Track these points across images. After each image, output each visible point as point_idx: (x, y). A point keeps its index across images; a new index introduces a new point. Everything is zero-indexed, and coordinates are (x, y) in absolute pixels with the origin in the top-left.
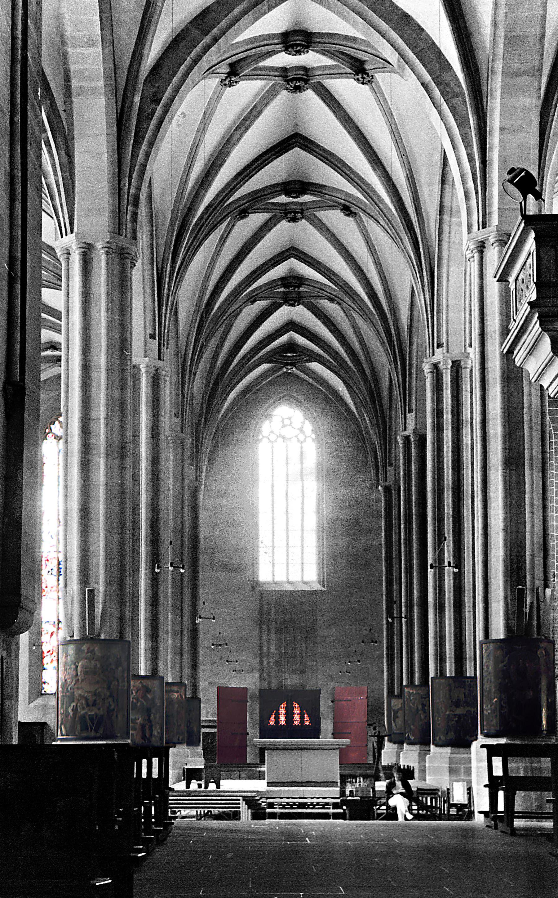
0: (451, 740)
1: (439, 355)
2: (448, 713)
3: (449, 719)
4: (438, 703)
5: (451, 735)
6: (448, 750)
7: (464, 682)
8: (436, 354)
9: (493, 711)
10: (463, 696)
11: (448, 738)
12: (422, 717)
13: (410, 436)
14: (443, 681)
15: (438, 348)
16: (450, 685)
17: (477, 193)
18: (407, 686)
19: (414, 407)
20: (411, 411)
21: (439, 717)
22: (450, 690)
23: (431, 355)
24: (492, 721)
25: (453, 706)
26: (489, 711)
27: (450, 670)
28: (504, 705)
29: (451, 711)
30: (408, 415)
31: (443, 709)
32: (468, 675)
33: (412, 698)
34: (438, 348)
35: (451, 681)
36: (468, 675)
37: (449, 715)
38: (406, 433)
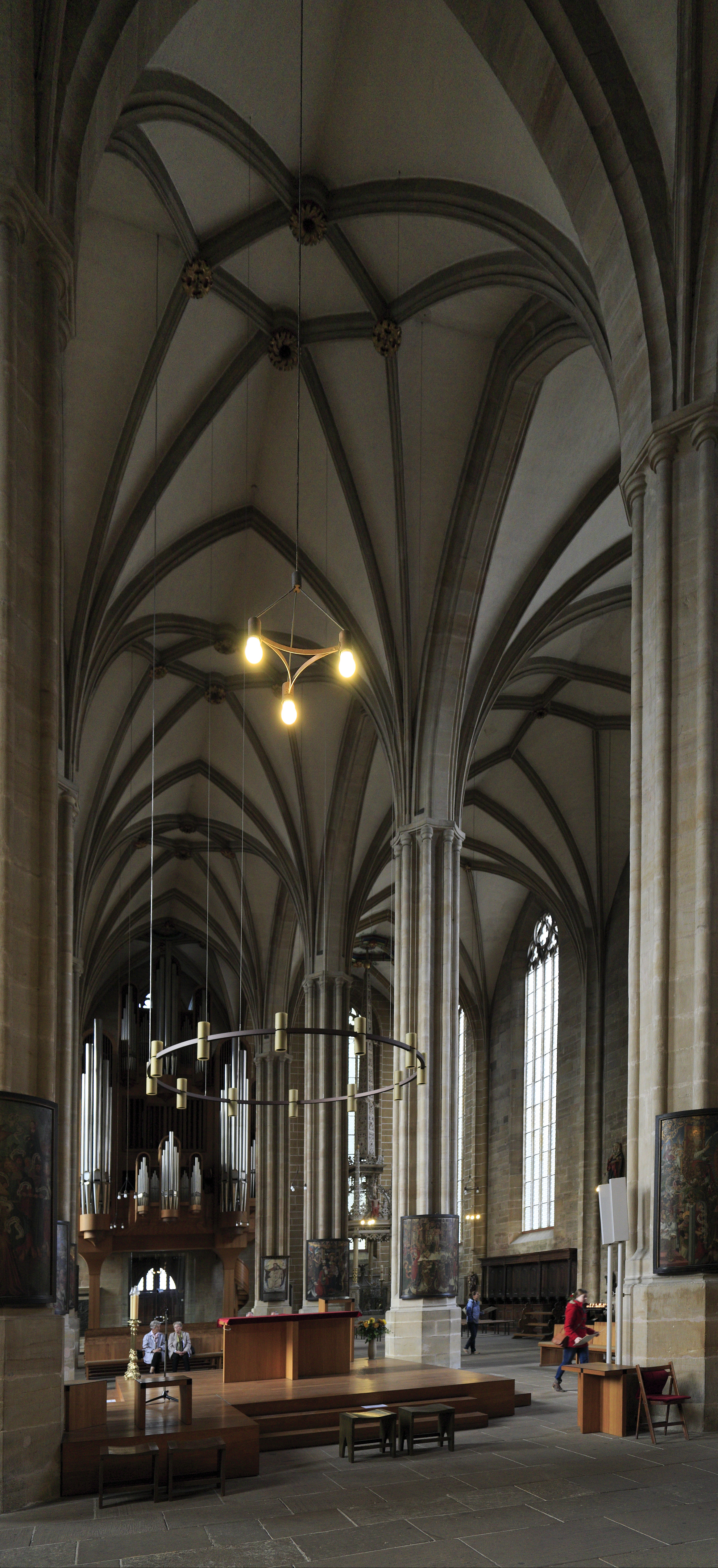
0: (423, 1292)
1: (418, 822)
2: (421, 1259)
3: (420, 1267)
4: (409, 1248)
5: (423, 1287)
6: (420, 1303)
7: (440, 1221)
8: (413, 821)
9: (681, 1233)
10: (438, 1238)
11: (420, 1290)
12: (326, 1272)
13: (318, 979)
14: (416, 1220)
15: (415, 815)
16: (424, 1225)
17: (674, 344)
18: (311, 1241)
19: (324, 948)
20: (320, 953)
21: (410, 1263)
22: (424, 1231)
23: (407, 822)
24: (678, 1250)
25: (428, 1251)
26: (674, 1234)
27: (422, 1208)
28: (700, 1222)
29: (424, 1257)
30: (317, 958)
31: (415, 1254)
32: (443, 1213)
33: (316, 1253)
34: (415, 815)
35: (426, 1220)
36: (443, 1213)
37: (421, 1262)
38: (315, 975)
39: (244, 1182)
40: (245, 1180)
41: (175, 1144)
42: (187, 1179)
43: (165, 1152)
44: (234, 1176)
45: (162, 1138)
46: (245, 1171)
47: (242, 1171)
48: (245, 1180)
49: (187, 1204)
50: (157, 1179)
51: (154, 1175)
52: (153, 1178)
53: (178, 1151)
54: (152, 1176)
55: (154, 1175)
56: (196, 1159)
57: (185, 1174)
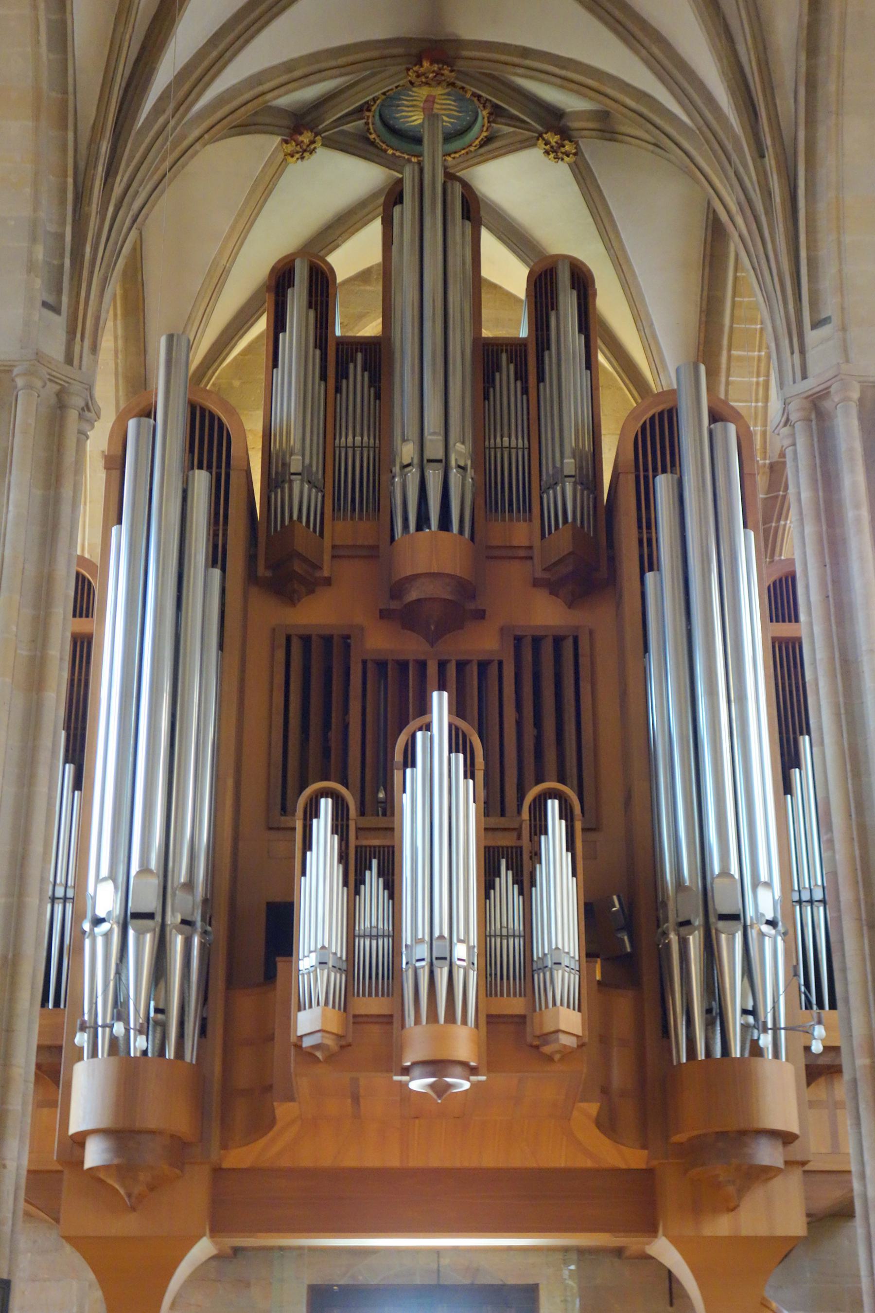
39: (765, 928)
40: (772, 923)
41: (458, 741)
42: (517, 901)
43: (415, 777)
44: (723, 904)
45: (403, 723)
46: (768, 885)
47: (755, 885)
48: (772, 923)
49: (515, 1005)
50: (383, 894)
51: (372, 878)
52: (365, 889)
53: (470, 773)
54: (360, 881)
55: (372, 878)
56: (553, 806)
57: (506, 878)
